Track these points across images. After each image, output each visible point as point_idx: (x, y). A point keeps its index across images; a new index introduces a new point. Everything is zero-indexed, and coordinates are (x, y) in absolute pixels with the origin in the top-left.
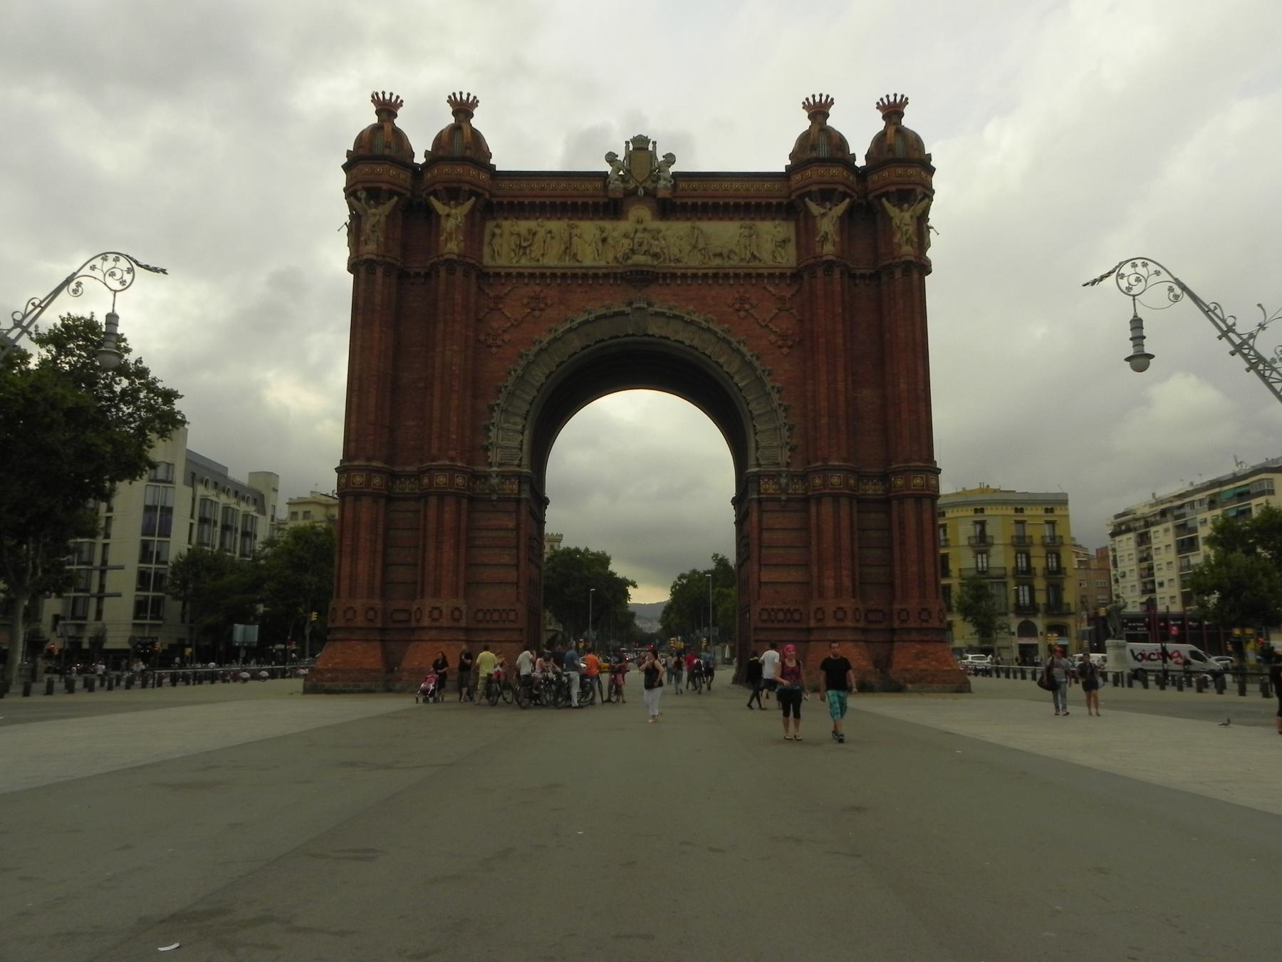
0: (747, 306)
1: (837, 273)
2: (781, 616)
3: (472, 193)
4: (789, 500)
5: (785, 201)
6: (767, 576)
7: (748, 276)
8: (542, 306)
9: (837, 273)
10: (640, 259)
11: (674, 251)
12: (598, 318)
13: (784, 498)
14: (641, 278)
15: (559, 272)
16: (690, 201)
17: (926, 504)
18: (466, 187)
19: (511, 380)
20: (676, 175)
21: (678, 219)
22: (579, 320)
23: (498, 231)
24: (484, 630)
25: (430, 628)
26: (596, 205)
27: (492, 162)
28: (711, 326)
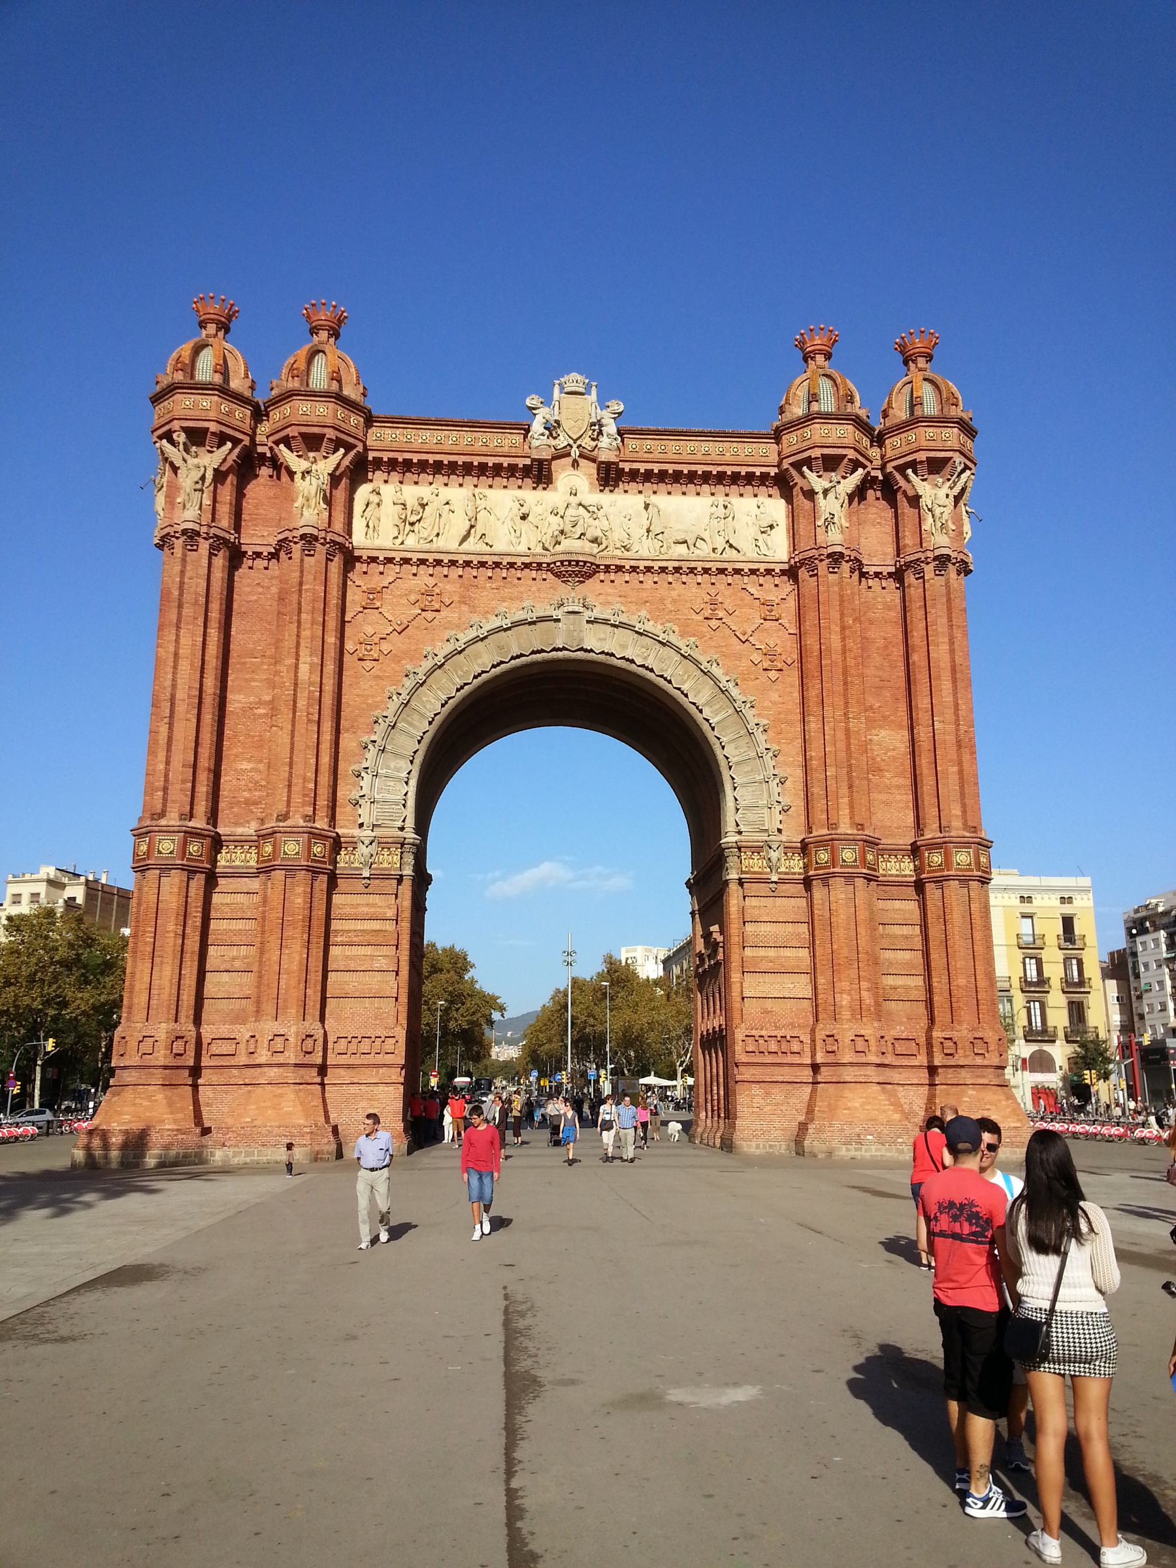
0: (721, 614)
1: (846, 567)
2: (773, 1047)
3: (338, 444)
4: (781, 881)
5: (773, 471)
7: (722, 571)
8: (437, 606)
9: (846, 567)
12: (516, 624)
14: (578, 571)
15: (461, 559)
18: (331, 434)
22: (487, 627)
23: (374, 499)
24: (349, 1067)
25: (270, 1065)
28: (673, 639)
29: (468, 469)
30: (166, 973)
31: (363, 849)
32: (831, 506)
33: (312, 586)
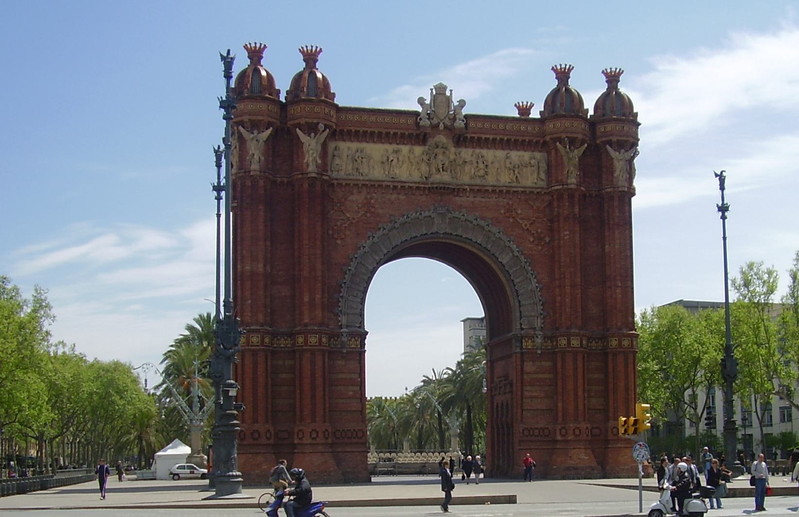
0: (514, 214)
13: (539, 352)
16: (476, 136)
17: (631, 356)
20: (467, 117)
21: (466, 147)
26: (410, 135)
27: (336, 102)
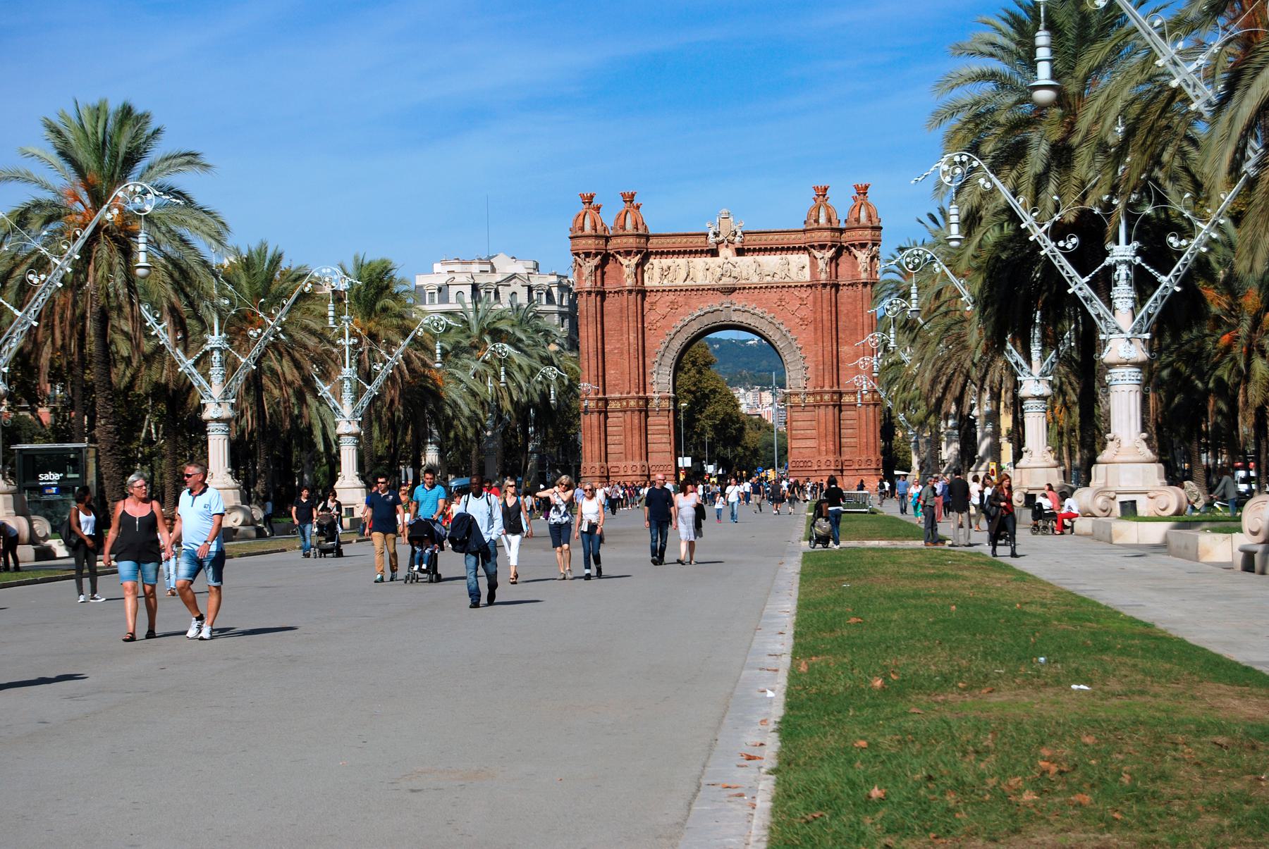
6: (795, 444)
10: (727, 281)
11: (744, 275)
19: (663, 347)
29: (685, 253)
30: (597, 446)
31: (656, 401)
32: (821, 264)
33: (632, 308)
